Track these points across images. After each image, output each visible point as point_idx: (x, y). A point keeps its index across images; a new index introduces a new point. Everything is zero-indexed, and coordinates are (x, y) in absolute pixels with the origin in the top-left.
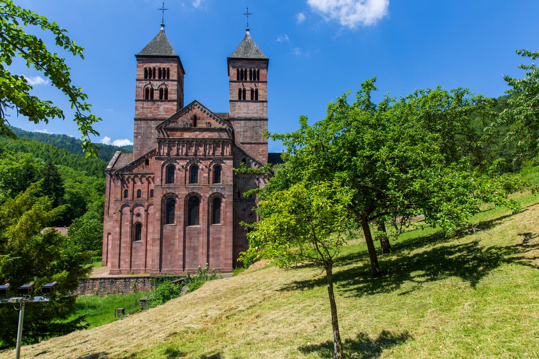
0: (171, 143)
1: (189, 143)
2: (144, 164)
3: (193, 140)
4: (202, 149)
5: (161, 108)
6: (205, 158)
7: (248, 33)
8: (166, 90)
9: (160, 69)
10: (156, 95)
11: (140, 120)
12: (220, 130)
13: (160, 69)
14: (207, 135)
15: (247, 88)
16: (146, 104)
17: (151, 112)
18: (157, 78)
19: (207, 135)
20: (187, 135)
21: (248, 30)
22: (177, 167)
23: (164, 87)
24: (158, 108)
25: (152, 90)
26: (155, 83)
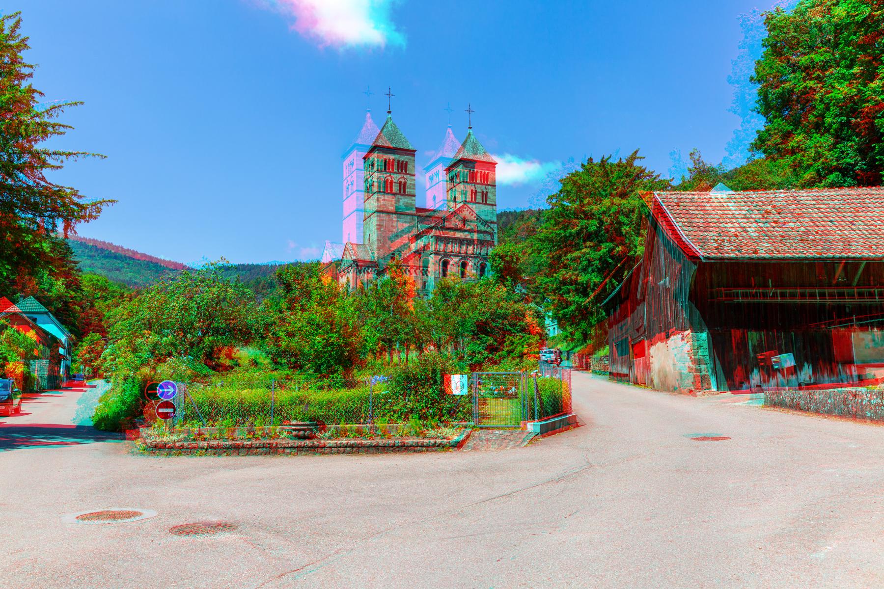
0: (446, 240)
1: (461, 241)
2: (417, 257)
3: (464, 240)
4: (471, 248)
5: (401, 203)
6: (474, 256)
7: (471, 131)
8: (405, 183)
9: (399, 161)
10: (395, 189)
11: (382, 212)
12: (485, 232)
13: (399, 161)
14: (475, 236)
15: (479, 190)
16: (387, 197)
17: (392, 205)
18: (396, 170)
19: (475, 236)
20: (459, 235)
21: (470, 128)
22: (452, 262)
23: (403, 180)
24: (398, 201)
25: (392, 183)
26: (394, 176)
